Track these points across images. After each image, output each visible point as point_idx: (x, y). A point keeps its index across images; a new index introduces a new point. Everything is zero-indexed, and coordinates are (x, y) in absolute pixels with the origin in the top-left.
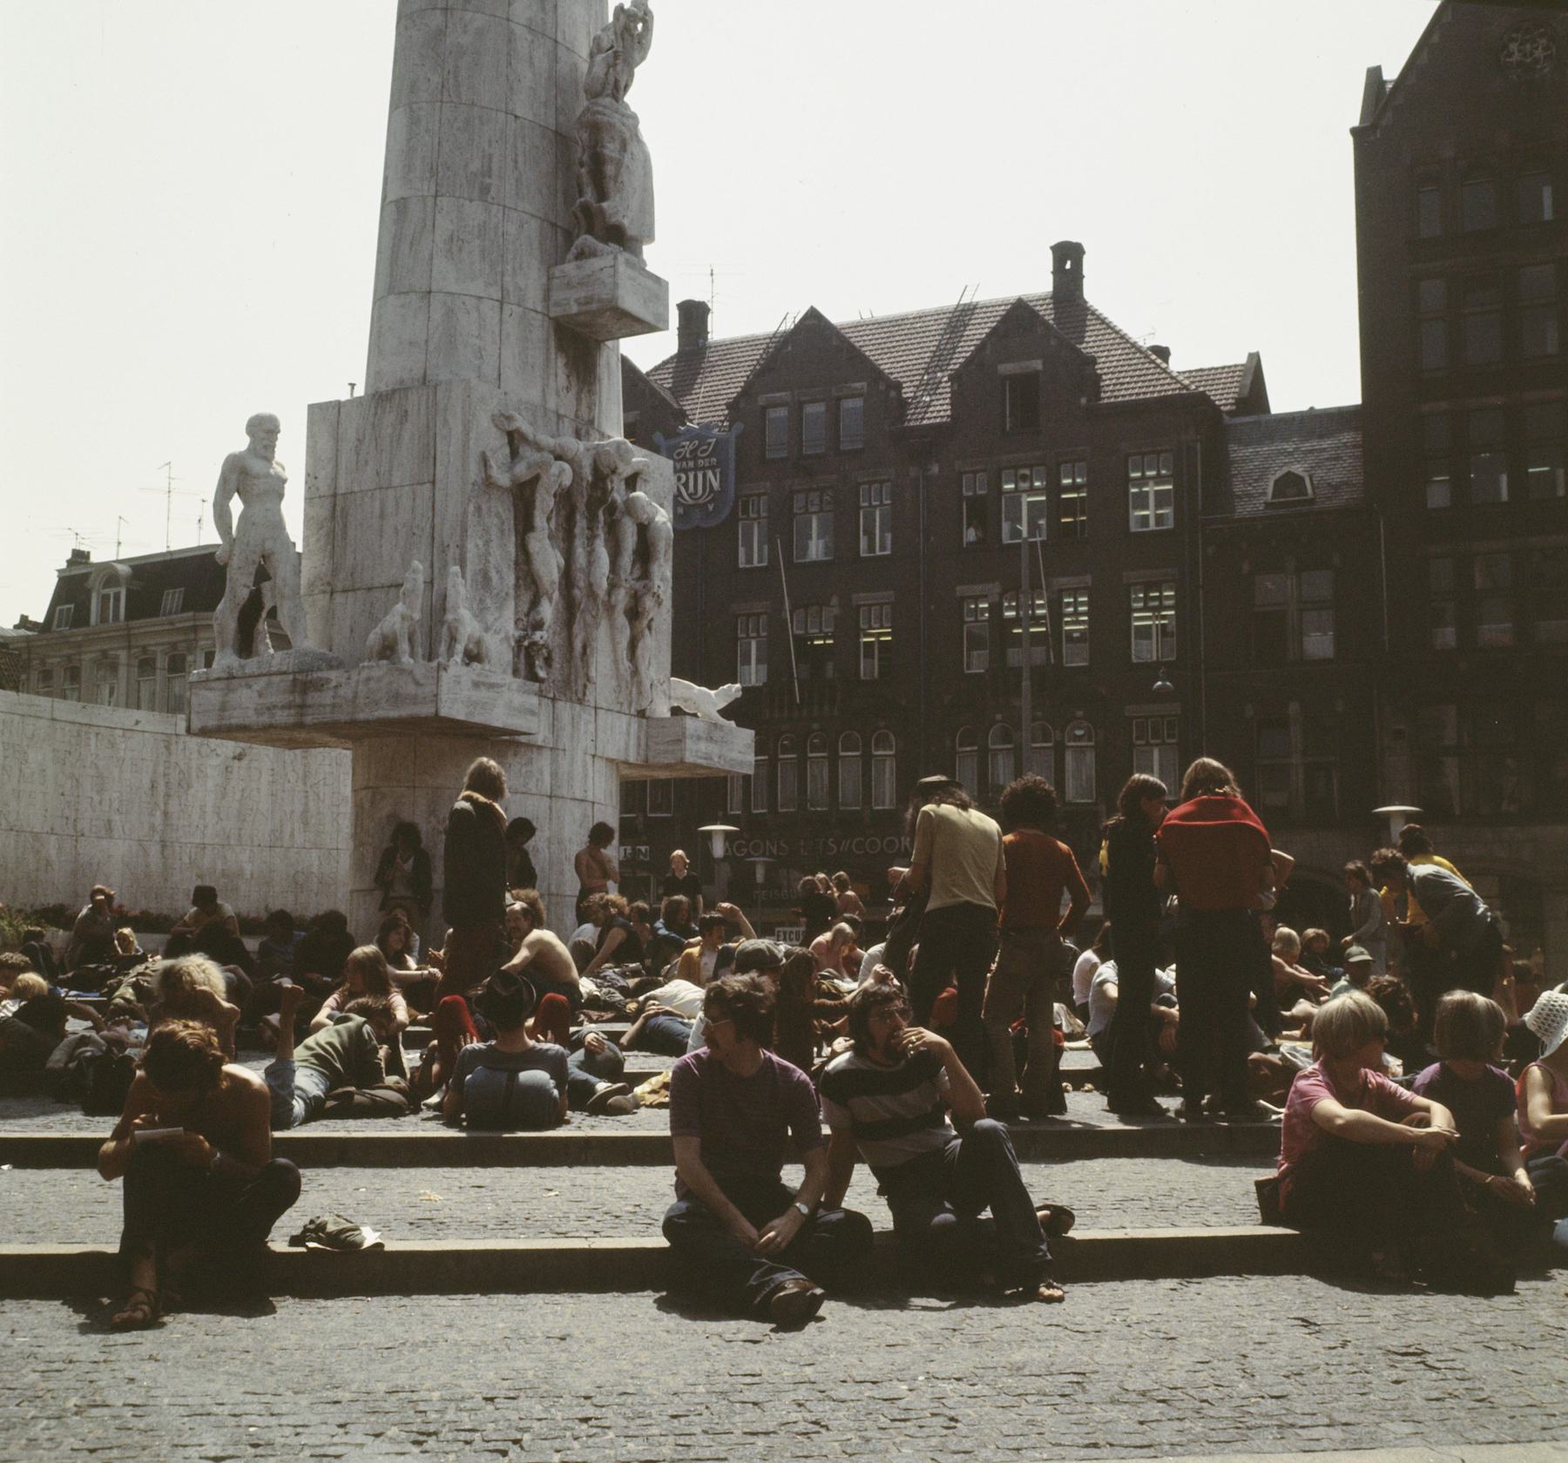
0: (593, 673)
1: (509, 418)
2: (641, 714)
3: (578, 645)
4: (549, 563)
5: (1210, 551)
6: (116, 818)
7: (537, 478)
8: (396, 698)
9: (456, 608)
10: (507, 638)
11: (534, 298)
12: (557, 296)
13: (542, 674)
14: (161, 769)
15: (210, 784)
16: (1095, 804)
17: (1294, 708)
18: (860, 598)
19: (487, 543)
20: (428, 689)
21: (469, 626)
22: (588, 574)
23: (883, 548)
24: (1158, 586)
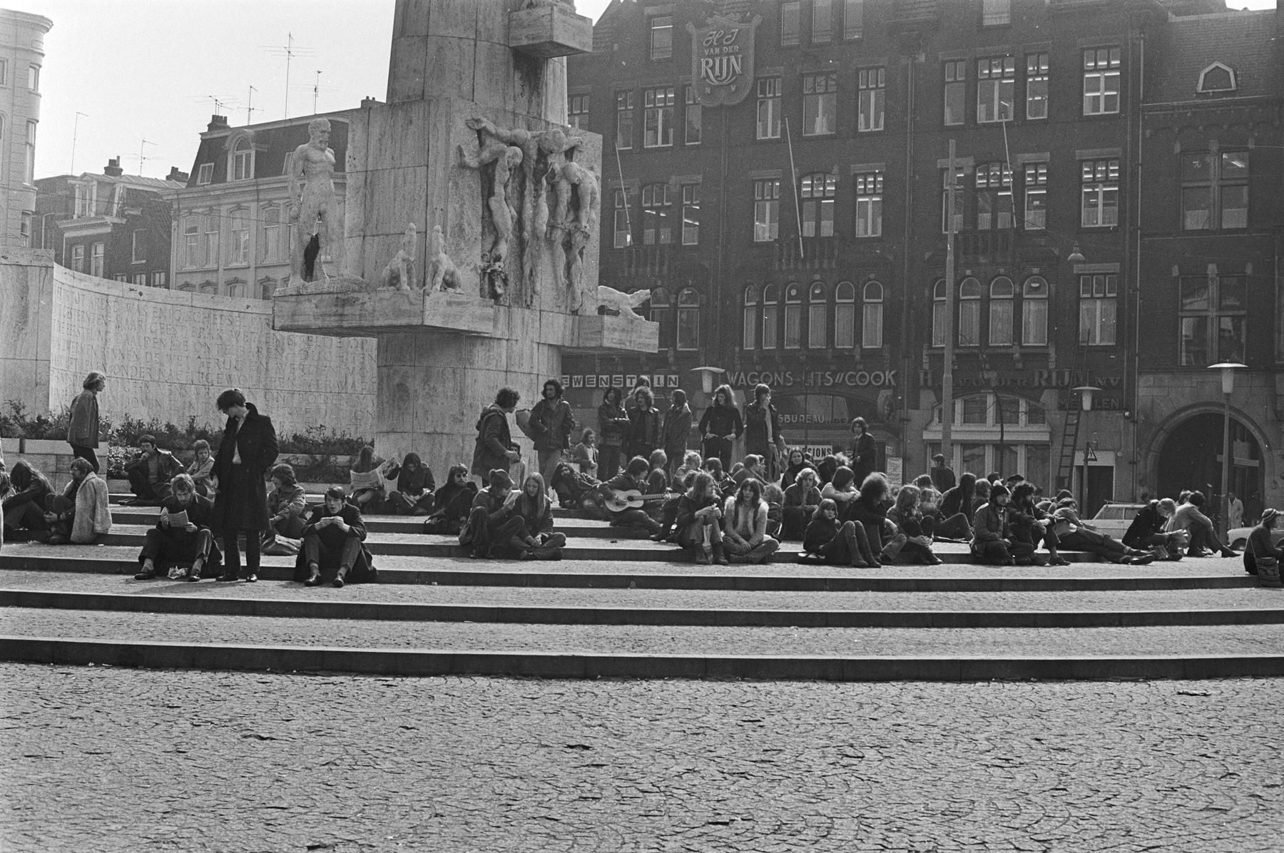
0: (538, 288)
1: (478, 121)
2: (575, 313)
3: (527, 271)
4: (505, 214)
5: (1148, 133)
6: (234, 373)
7: (496, 161)
8: (399, 313)
9: (437, 253)
10: (475, 268)
11: (498, 35)
12: (514, 33)
13: (500, 291)
14: (264, 339)
15: (297, 349)
16: (1046, 347)
17: (1212, 269)
18: (857, 168)
19: (462, 206)
20: (417, 308)
21: (446, 263)
22: (534, 221)
23: (877, 125)
24: (1106, 161)
